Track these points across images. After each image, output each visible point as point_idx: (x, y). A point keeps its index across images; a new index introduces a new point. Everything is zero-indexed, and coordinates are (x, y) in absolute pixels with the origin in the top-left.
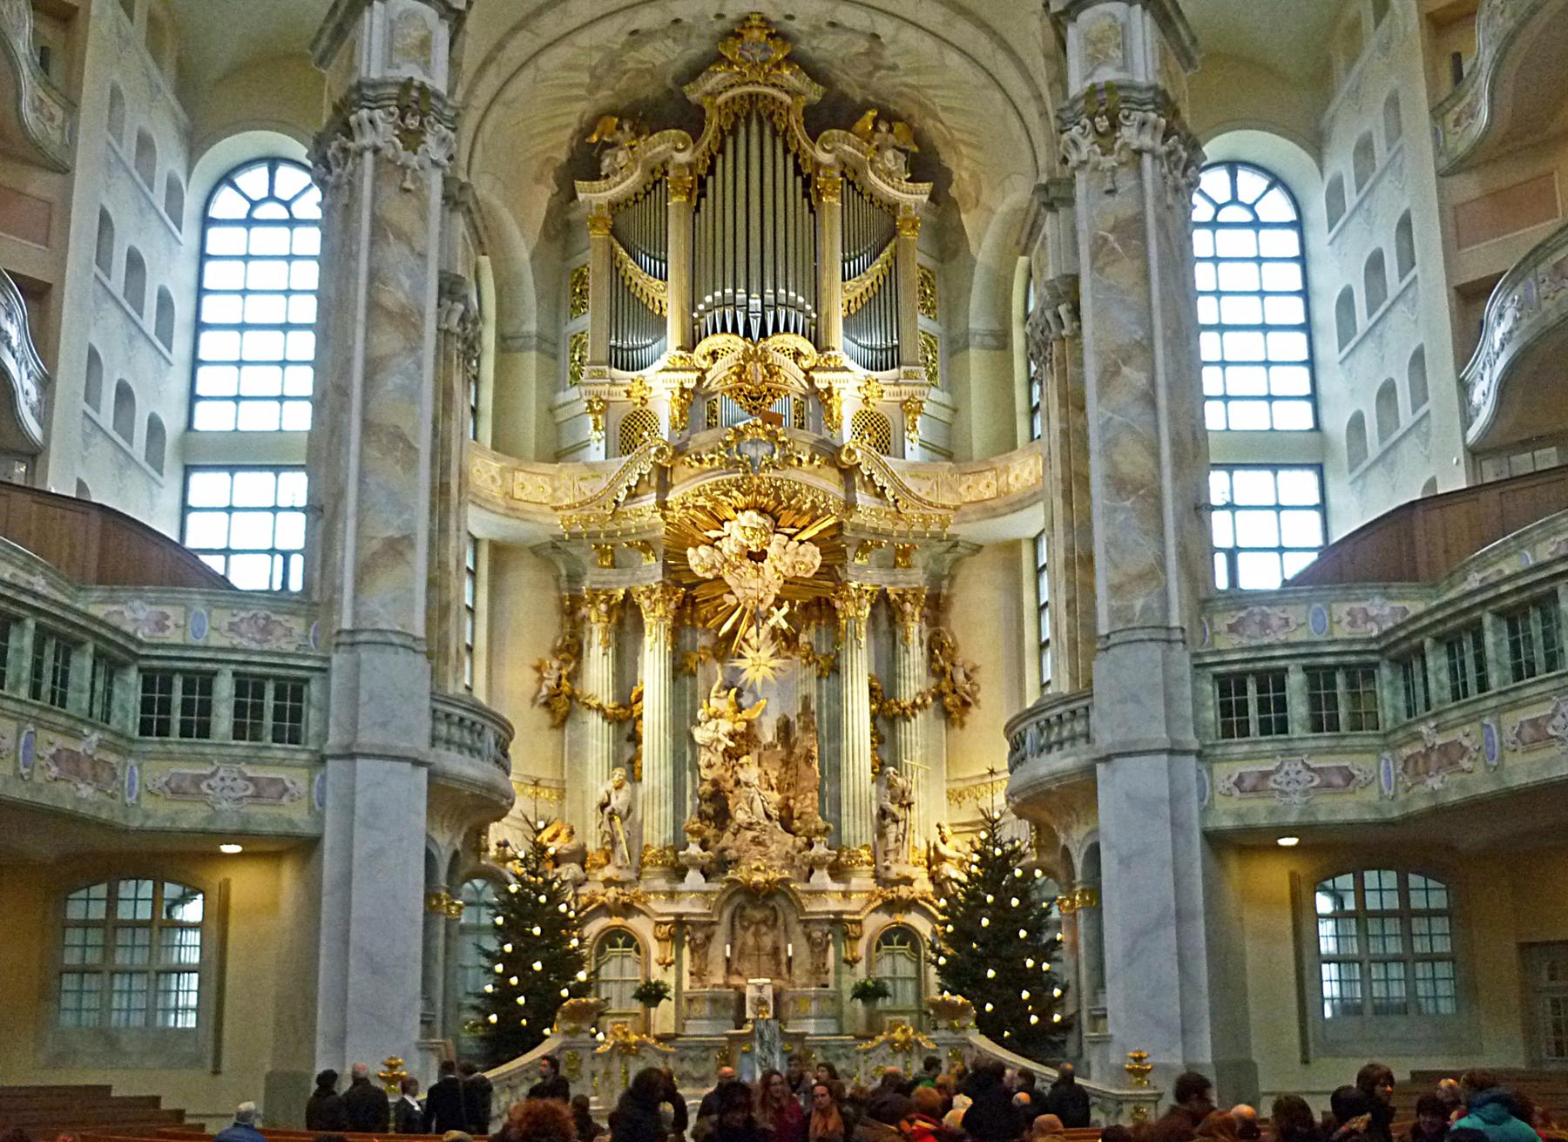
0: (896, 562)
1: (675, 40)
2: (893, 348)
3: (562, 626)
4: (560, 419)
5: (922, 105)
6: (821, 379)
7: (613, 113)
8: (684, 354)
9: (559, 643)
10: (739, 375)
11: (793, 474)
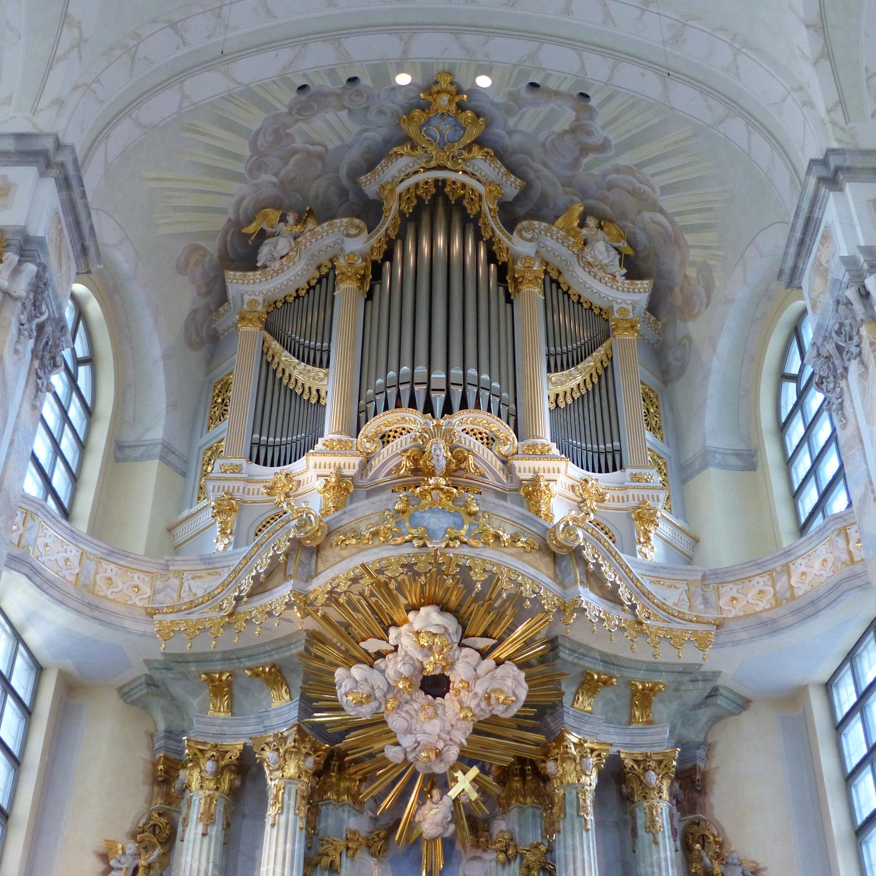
0: (632, 716)
1: (351, 112)
2: (613, 452)
3: (150, 800)
4: (180, 540)
5: (634, 193)
6: (524, 468)
7: (278, 209)
8: (344, 438)
9: (143, 821)
10: (415, 461)
11: (490, 554)
